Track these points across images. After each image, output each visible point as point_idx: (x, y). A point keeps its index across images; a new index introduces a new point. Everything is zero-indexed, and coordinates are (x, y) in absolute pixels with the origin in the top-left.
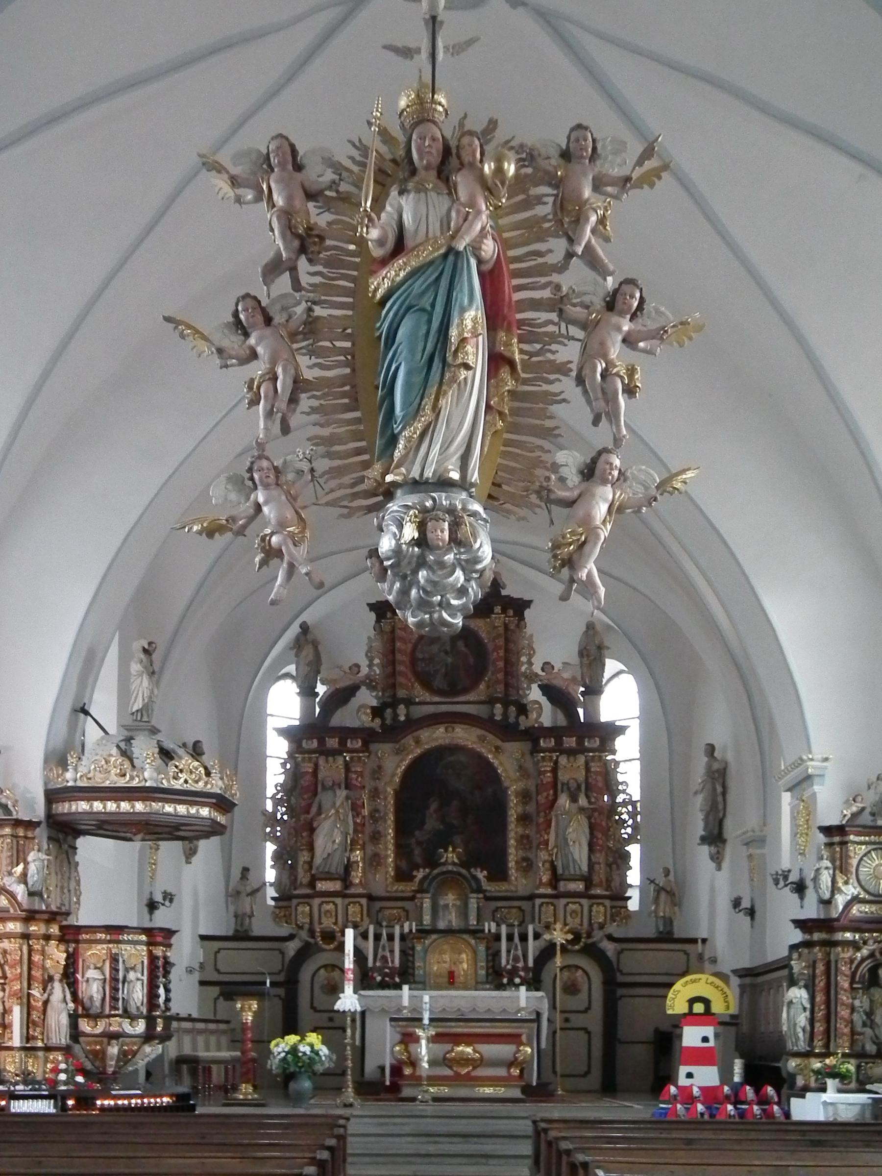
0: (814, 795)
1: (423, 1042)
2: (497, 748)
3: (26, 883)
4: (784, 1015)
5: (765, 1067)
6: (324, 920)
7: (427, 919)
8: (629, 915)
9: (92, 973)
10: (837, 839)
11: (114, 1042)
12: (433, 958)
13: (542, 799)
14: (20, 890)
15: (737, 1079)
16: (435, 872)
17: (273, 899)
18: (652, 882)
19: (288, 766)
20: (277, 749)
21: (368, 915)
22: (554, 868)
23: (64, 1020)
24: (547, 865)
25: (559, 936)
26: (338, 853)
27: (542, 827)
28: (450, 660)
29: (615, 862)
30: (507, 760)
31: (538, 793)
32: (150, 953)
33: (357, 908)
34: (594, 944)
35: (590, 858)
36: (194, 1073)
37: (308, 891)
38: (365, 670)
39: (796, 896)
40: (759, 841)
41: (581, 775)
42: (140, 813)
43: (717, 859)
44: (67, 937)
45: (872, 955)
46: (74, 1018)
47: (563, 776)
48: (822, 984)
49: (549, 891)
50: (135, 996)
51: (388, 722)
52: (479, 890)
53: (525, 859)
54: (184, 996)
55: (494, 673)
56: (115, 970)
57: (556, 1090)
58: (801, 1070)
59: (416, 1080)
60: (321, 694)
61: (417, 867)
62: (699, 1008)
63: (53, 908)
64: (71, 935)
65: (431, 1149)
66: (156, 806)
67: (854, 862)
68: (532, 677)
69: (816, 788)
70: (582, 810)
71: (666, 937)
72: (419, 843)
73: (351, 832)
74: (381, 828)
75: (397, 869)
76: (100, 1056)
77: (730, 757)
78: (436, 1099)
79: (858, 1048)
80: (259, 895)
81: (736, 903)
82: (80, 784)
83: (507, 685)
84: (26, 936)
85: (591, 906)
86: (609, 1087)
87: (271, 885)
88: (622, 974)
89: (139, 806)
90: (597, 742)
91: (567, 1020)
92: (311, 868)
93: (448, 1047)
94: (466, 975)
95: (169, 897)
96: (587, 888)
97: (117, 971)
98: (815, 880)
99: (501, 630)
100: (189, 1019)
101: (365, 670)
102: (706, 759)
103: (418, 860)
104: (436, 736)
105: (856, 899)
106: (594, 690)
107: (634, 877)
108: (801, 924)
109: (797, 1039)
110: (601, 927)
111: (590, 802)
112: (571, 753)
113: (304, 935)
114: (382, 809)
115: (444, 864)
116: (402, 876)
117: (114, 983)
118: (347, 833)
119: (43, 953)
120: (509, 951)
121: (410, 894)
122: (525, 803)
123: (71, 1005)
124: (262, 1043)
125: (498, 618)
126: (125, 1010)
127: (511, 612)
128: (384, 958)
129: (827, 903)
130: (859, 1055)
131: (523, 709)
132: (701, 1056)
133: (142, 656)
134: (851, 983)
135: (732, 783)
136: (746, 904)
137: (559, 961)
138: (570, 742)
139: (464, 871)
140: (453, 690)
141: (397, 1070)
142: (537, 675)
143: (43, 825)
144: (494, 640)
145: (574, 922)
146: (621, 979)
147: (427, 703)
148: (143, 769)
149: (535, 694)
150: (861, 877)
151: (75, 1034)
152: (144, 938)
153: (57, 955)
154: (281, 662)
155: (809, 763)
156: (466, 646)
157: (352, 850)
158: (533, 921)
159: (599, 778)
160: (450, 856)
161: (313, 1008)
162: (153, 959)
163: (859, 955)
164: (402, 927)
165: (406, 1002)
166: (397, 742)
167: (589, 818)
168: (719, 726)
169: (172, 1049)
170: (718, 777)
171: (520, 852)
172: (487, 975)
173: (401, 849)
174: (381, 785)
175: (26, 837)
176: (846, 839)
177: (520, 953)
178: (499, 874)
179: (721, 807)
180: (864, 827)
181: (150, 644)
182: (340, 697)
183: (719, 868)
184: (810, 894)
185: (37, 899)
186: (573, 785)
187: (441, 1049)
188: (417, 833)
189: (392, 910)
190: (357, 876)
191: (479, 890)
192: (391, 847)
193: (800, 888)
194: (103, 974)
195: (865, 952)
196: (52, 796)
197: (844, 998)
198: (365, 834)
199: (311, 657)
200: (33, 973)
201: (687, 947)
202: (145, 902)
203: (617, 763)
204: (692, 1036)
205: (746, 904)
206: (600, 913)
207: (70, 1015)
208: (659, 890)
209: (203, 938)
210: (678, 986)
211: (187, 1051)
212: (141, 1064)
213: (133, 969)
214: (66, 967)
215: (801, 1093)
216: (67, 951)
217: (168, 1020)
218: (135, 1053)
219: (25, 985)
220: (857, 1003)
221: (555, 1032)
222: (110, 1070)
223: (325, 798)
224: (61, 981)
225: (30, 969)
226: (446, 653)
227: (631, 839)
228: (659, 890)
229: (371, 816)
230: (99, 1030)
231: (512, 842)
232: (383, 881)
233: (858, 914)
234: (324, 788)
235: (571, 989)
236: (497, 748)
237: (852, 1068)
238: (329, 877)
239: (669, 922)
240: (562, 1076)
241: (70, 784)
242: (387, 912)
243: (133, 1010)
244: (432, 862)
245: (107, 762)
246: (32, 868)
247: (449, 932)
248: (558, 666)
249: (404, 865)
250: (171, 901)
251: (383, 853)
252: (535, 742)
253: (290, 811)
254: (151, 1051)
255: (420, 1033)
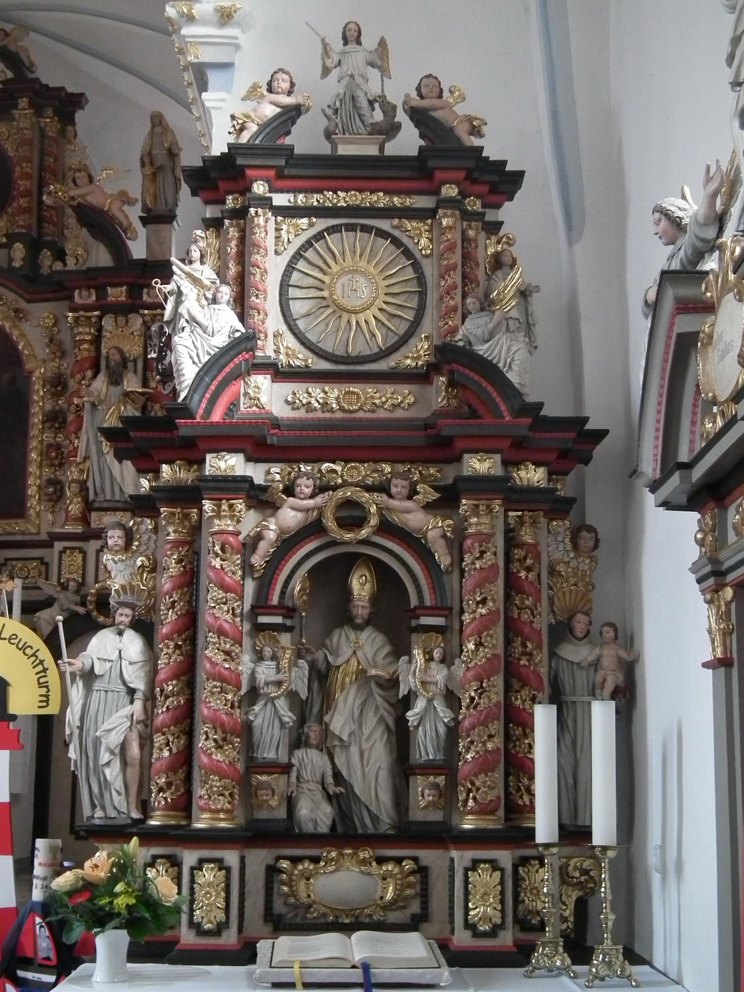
2: (17, 311)
236: (17, 311)
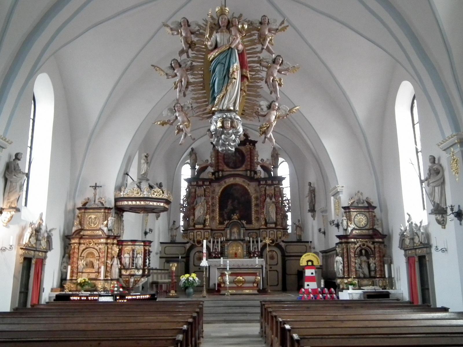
0: (340, 197)
1: (227, 276)
2: (249, 184)
3: (107, 227)
4: (335, 265)
5: (331, 282)
6: (197, 237)
7: (228, 236)
8: (288, 234)
9: (126, 255)
10: (347, 210)
11: (132, 277)
12: (230, 248)
13: (261, 199)
14: (105, 229)
15: (322, 286)
16: (231, 222)
17: (182, 230)
18: (295, 224)
19: (187, 190)
20: (184, 185)
21: (211, 235)
22: (266, 220)
23: (117, 270)
24: (264, 219)
25: (268, 241)
26: (202, 216)
27: (262, 207)
28: (234, 158)
29: (284, 218)
30: (251, 188)
31: (261, 197)
32: (144, 248)
33: (208, 233)
34: (278, 244)
35: (276, 217)
36: (157, 287)
37: (193, 228)
38: (210, 162)
39: (336, 228)
40: (325, 211)
41: (273, 192)
42: (143, 205)
43: (313, 216)
44: (119, 244)
45: (360, 246)
46: (120, 270)
47: (268, 192)
48: (346, 255)
49: (265, 227)
50: (139, 262)
51: (217, 176)
52: (244, 227)
53: (257, 217)
54: (154, 262)
55: (247, 162)
56: (133, 254)
57: (268, 290)
58: (341, 283)
59: (225, 288)
60: (197, 168)
61: (225, 220)
62: (310, 263)
63: (116, 235)
64: (120, 243)
65: (230, 311)
66: (147, 203)
67: (353, 217)
68: (258, 163)
69: (341, 195)
70: (273, 202)
71: (299, 241)
72: (226, 213)
73: (206, 209)
74: (214, 208)
75: (220, 221)
76: (128, 282)
77: (316, 186)
78: (231, 294)
79: (358, 276)
80: (178, 229)
81: (320, 230)
82: (125, 196)
83: (251, 165)
84: (107, 244)
85: (277, 232)
86: (284, 289)
87: (182, 226)
88: (287, 253)
89: (142, 203)
90: (277, 182)
91: (271, 268)
92: (194, 221)
93: (235, 277)
94: (240, 254)
95: (151, 230)
96: (276, 226)
97: (134, 254)
98: (342, 223)
99: (249, 150)
100: (156, 269)
101: (210, 162)
102: (309, 187)
103: (226, 218)
104: (231, 181)
105: (354, 229)
106: (276, 167)
107: (289, 222)
108: (339, 237)
109: (340, 273)
110: (280, 238)
111: (276, 200)
112: (270, 185)
113: (192, 242)
114: (215, 202)
115: (233, 219)
116: (221, 223)
117: (133, 258)
118: (205, 210)
119: (112, 249)
120: (253, 246)
121: (223, 229)
122: (257, 201)
123: (120, 266)
124: (178, 277)
125: (248, 146)
126: (136, 267)
127: (252, 144)
128: (216, 249)
129: (346, 230)
130: (358, 278)
131: (256, 173)
132: (311, 279)
133: (145, 158)
134: (355, 255)
135: (316, 194)
136: (322, 230)
137: (268, 249)
138: (269, 182)
139: (239, 221)
140: (235, 167)
141: (219, 285)
142: (259, 163)
143: (114, 209)
144: (247, 152)
145: (272, 237)
146: (286, 254)
147: (228, 171)
148: (144, 192)
149: (259, 168)
150: (355, 222)
151: (120, 275)
152: (142, 244)
153: (116, 249)
154: (186, 159)
155: (338, 188)
156: (239, 154)
157: (206, 215)
158: (260, 236)
159: (278, 193)
160: (235, 217)
161: (194, 265)
162: (145, 250)
163: (356, 246)
164: (221, 239)
165: (222, 263)
166: (219, 182)
167: (275, 205)
168: (312, 177)
169: (150, 279)
170: (313, 192)
171: (256, 215)
172: (247, 254)
173: (221, 215)
174: (214, 195)
175: (108, 213)
176: (350, 210)
177: (256, 246)
178: (250, 222)
179: (314, 201)
180: (356, 207)
181: (147, 154)
182: (203, 169)
183: (314, 219)
184: (341, 227)
185: (110, 232)
186: (271, 195)
187: (233, 278)
188: (225, 210)
189: (218, 234)
190: (207, 223)
191: (244, 227)
192: (218, 214)
193: (338, 226)
194: (130, 255)
195: (358, 245)
196: (117, 200)
197: (353, 260)
198: (210, 210)
199: (194, 158)
200: (108, 255)
201: (306, 244)
202: (144, 232)
203: (283, 188)
204: (308, 273)
205: (322, 230)
206: (280, 234)
207: (119, 269)
208: (297, 226)
209: (161, 243)
210: (303, 257)
211: (155, 280)
212: (140, 284)
213: (139, 253)
214: (119, 253)
215: (342, 290)
216: (119, 248)
217: (149, 270)
218: (139, 281)
219: (106, 259)
220: (357, 261)
221: (267, 272)
222: (131, 286)
223: (198, 200)
224: (117, 258)
225: (107, 254)
226: (233, 156)
227: (288, 211)
228: (297, 226)
229: (212, 205)
230: (128, 273)
231: (253, 212)
232: (215, 224)
233: (355, 234)
234: (198, 197)
235: (272, 258)
237: (356, 282)
238: (199, 224)
239: (300, 236)
240: (270, 286)
241: (122, 196)
242: (216, 234)
243: (138, 267)
244: (230, 218)
245: (133, 189)
246: (110, 222)
247: (235, 240)
248: (265, 160)
249: (221, 219)
250: (152, 232)
251: (215, 216)
252: (259, 182)
253: (188, 203)
254: (144, 280)
255: (226, 273)
